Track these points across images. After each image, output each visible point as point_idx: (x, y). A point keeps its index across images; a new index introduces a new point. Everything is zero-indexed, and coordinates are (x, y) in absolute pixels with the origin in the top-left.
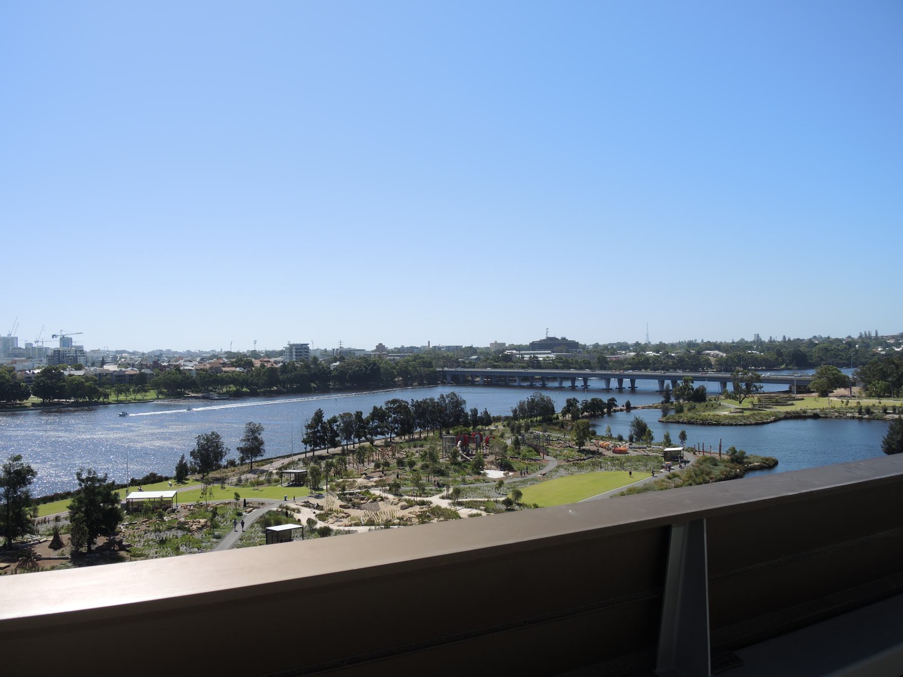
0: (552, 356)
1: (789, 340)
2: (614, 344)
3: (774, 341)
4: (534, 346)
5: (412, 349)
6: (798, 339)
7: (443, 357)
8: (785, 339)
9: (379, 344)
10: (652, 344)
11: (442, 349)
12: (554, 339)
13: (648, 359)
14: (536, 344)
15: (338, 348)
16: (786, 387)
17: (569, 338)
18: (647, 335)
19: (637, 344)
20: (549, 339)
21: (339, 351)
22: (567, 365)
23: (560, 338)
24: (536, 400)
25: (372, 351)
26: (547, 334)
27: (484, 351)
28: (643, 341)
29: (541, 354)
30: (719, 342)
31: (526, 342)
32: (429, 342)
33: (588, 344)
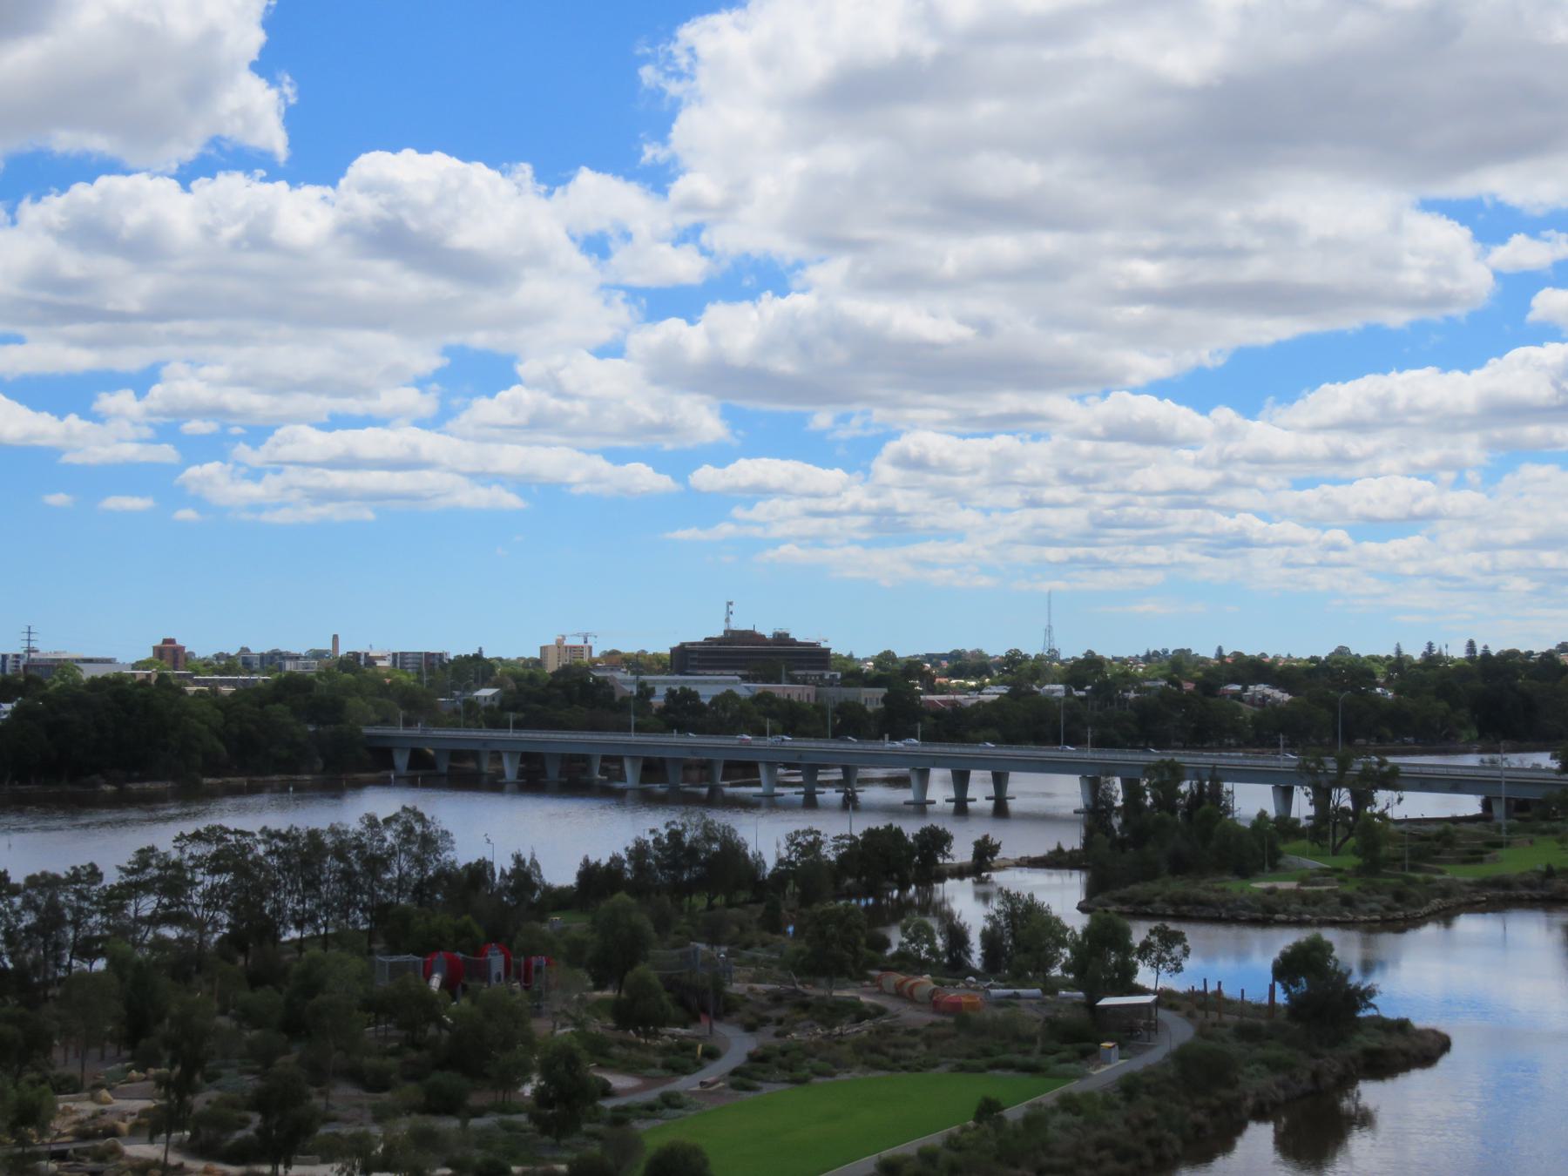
0: (744, 690)
1: (1486, 655)
2: (943, 657)
3: (1440, 657)
4: (686, 658)
5: (273, 659)
6: (1513, 654)
7: (384, 690)
8: (1475, 652)
9: (166, 641)
10: (1062, 657)
11: (380, 663)
12: (750, 637)
13: (1047, 702)
14: (693, 652)
15: (21, 652)
16: (1469, 805)
17: (801, 634)
18: (1049, 630)
19: (1014, 660)
20: (733, 637)
21: (22, 663)
22: (793, 719)
23: (768, 634)
24: (687, 838)
25: (135, 666)
26: (727, 620)
27: (520, 670)
28: (1032, 648)
29: (706, 682)
30: (1271, 657)
31: (662, 645)
32: (335, 638)
33: (858, 655)
